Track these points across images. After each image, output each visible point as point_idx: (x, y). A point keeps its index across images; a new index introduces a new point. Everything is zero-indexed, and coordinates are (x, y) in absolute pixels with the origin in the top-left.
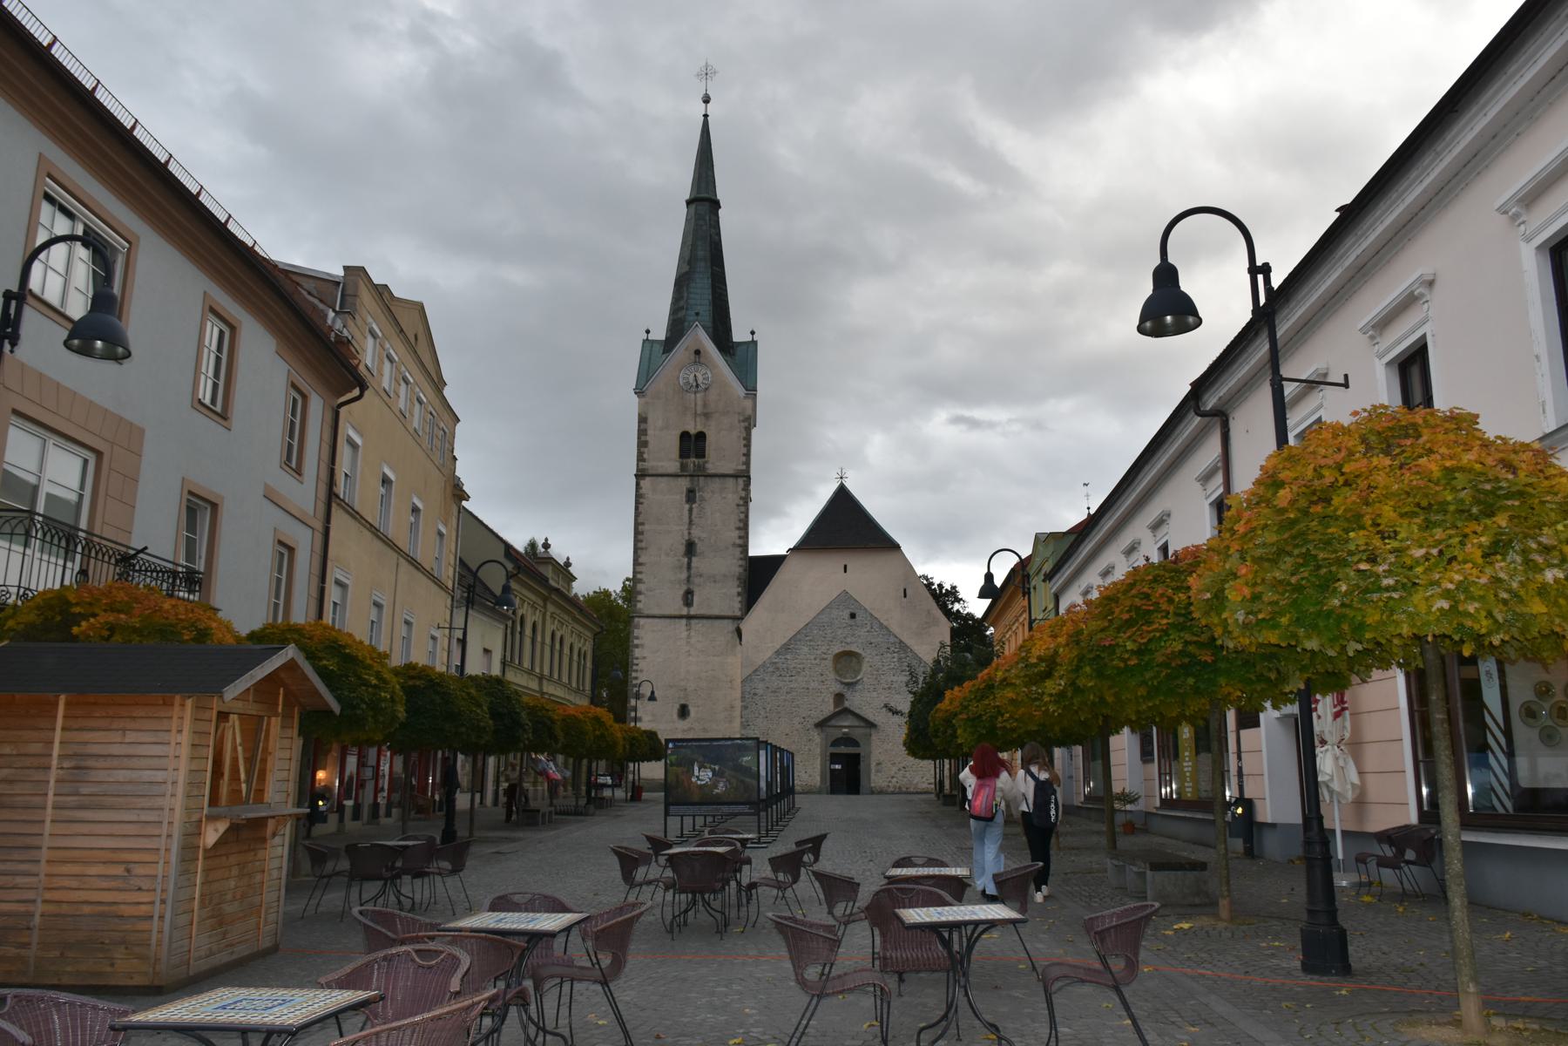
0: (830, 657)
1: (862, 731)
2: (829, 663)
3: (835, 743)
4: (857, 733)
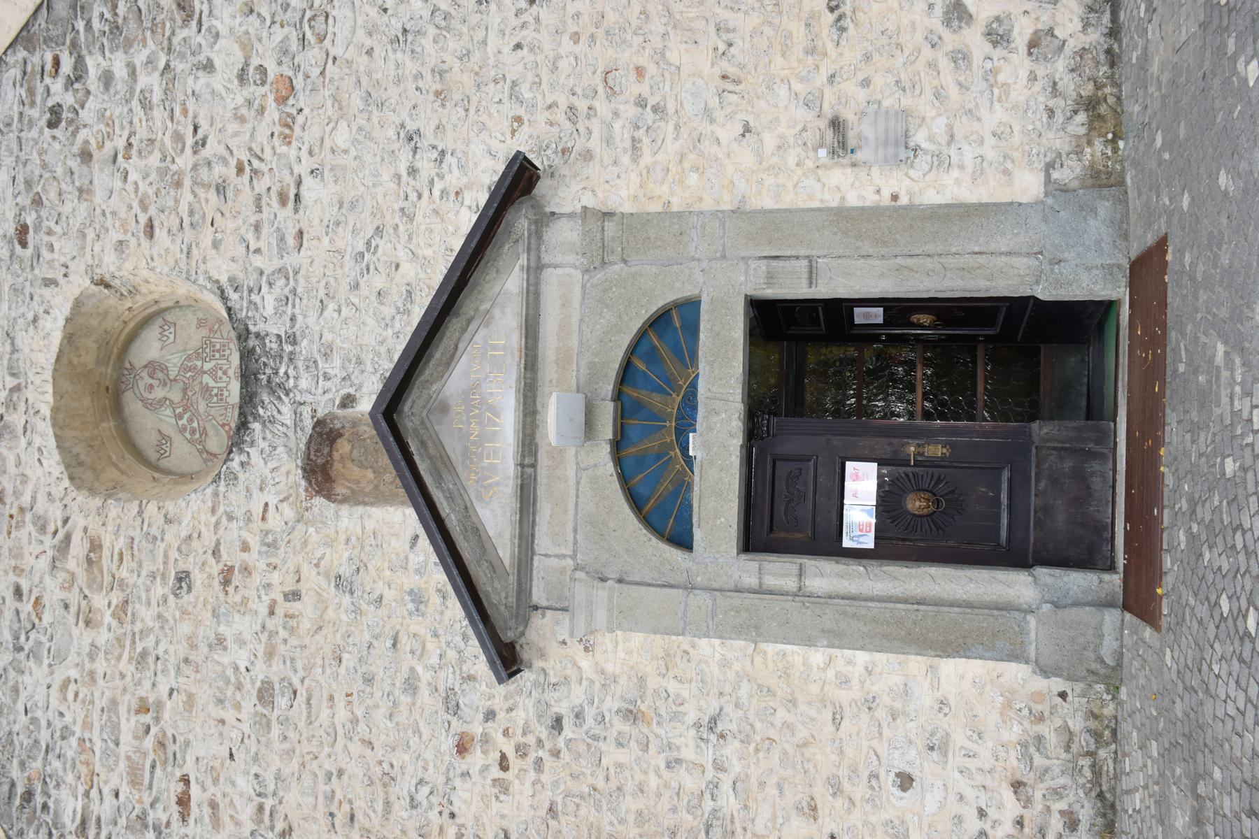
0: (85, 513)
1: (565, 284)
2: (114, 521)
3: (664, 515)
4: (574, 311)
